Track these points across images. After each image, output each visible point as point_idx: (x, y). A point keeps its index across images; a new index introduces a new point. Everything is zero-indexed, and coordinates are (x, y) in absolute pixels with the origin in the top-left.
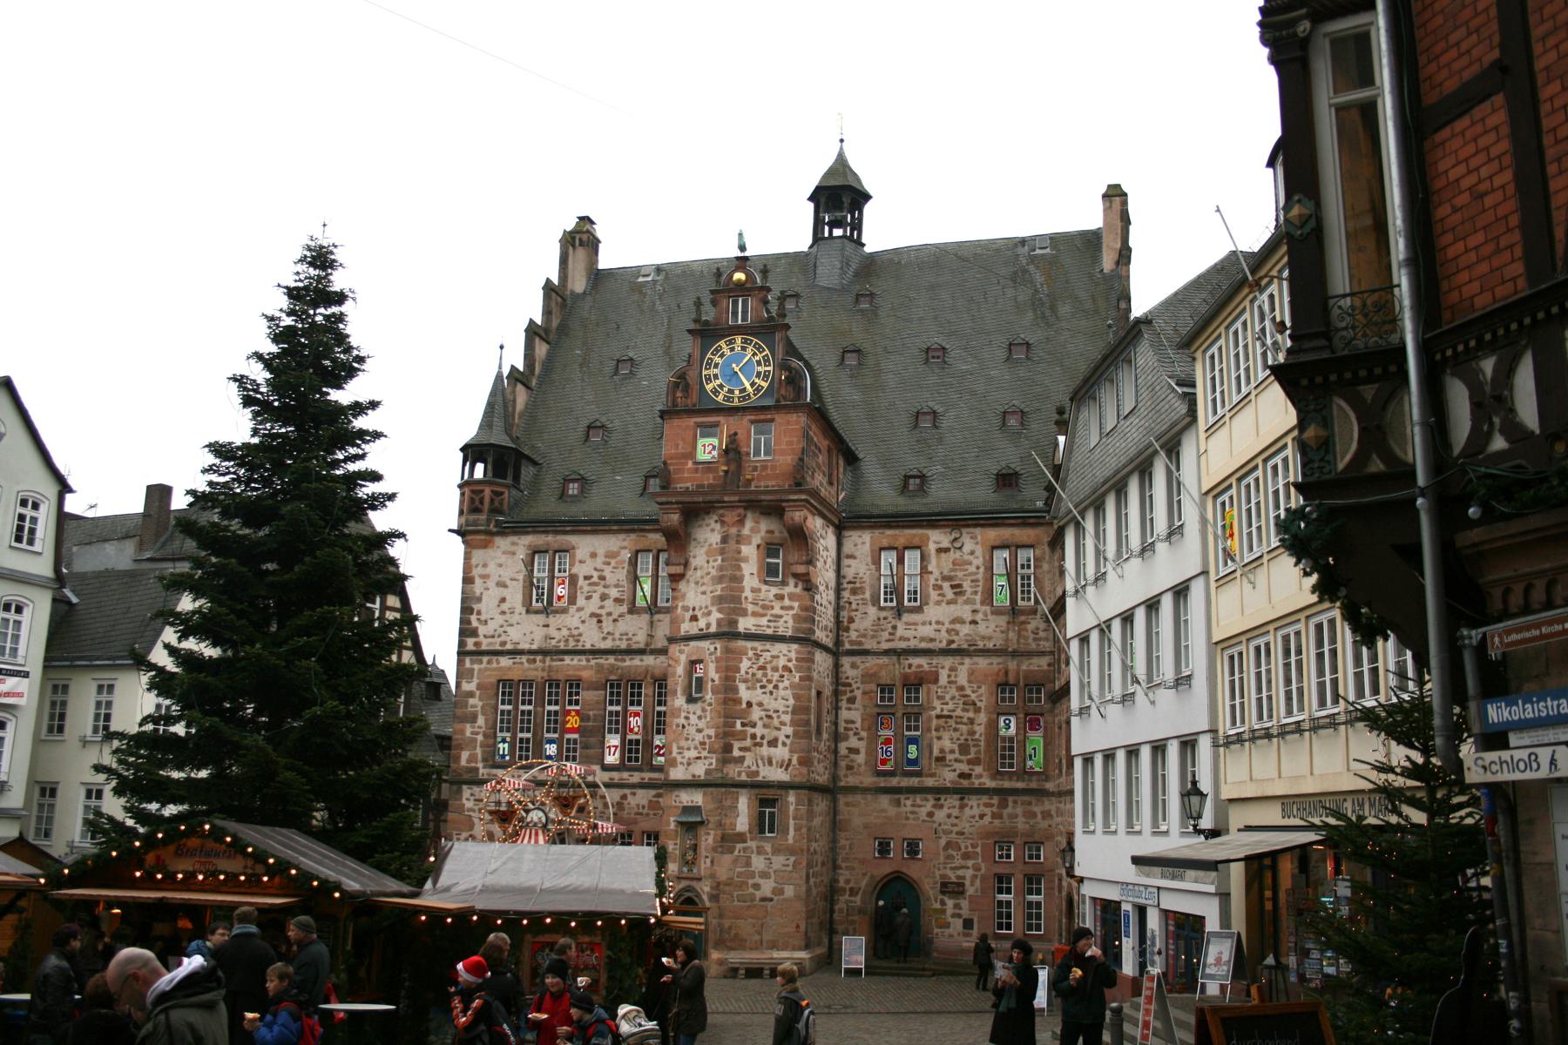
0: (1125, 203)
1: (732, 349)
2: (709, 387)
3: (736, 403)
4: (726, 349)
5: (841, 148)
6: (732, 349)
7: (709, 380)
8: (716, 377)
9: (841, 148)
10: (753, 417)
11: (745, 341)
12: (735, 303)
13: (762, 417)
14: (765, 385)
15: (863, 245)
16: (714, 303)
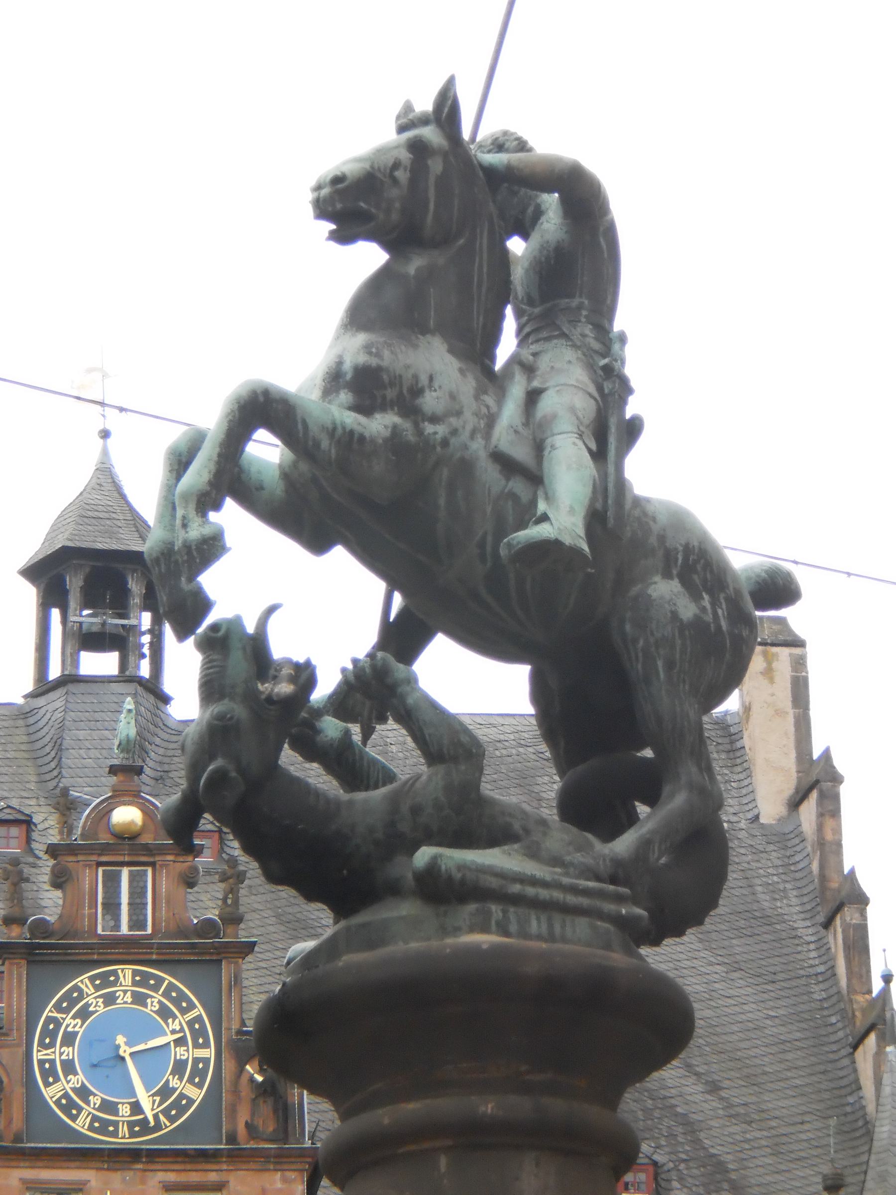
0: (799, 664)
1: (110, 999)
2: (51, 1093)
3: (123, 1138)
4: (93, 999)
5: (105, 452)
6: (110, 999)
7: (50, 1074)
8: (69, 1067)
9: (105, 452)
10: (171, 1177)
11: (143, 980)
12: (112, 881)
13: (194, 1177)
14: (196, 1094)
15: (165, 699)
16: (60, 880)
